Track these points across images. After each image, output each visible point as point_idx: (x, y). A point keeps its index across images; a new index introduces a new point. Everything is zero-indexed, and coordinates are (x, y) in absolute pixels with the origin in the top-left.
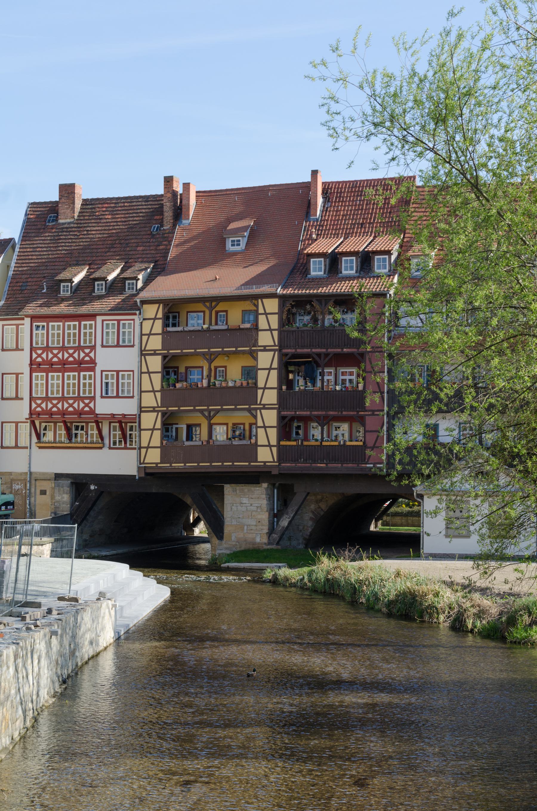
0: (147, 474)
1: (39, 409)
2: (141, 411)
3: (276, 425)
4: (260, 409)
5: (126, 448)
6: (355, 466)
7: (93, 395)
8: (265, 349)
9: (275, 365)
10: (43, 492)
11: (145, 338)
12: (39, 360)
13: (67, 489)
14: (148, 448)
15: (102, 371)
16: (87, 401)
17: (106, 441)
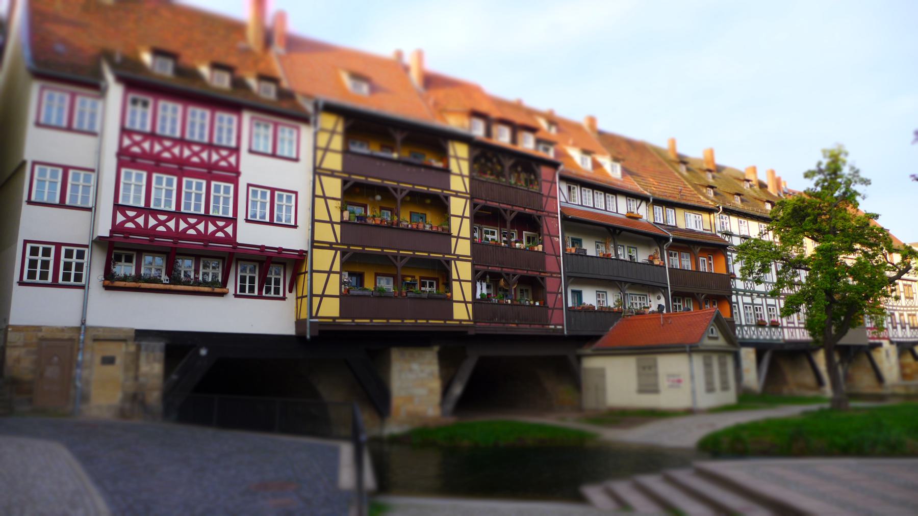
0: (320, 332)
1: (130, 225)
2: (313, 247)
3: (470, 279)
4: (455, 260)
5: (260, 297)
6: (540, 327)
7: (231, 215)
8: (457, 194)
9: (467, 214)
10: (109, 361)
11: (320, 154)
12: (136, 149)
13: (160, 354)
14: (322, 296)
15: (249, 185)
16: (221, 224)
17: (231, 287)
